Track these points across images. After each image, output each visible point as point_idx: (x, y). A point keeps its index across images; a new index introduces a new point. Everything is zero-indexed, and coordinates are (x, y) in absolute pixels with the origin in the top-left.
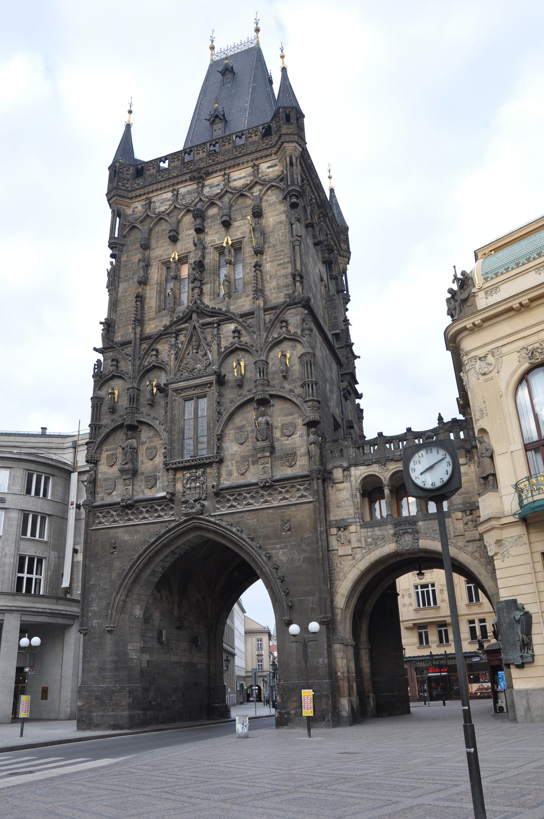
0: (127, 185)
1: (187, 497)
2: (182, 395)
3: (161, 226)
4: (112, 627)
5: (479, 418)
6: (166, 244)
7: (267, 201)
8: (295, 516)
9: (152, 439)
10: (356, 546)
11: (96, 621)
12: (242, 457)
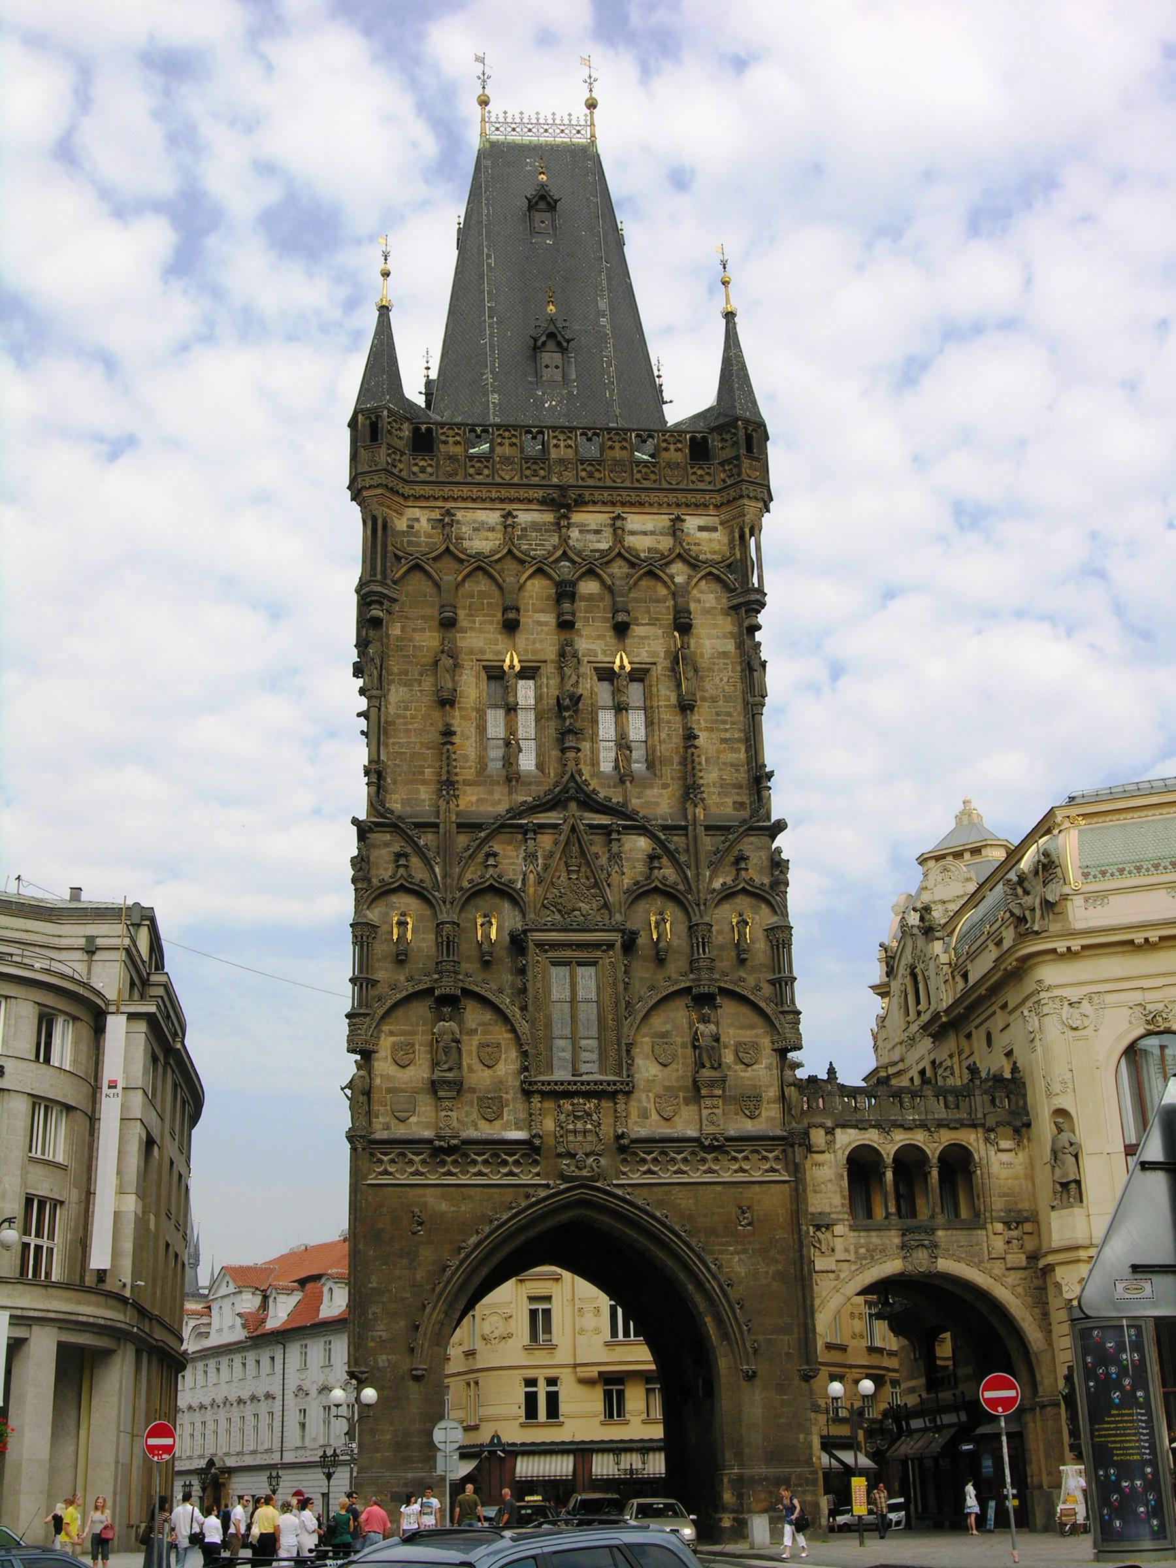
0: (401, 466)
2: (550, 954)
3: (478, 583)
4: (425, 1370)
5: (1059, 1092)
6: (491, 628)
7: (699, 601)
8: (759, 1202)
9: (491, 1028)
10: (843, 1259)
11: (384, 1357)
12: (667, 1088)
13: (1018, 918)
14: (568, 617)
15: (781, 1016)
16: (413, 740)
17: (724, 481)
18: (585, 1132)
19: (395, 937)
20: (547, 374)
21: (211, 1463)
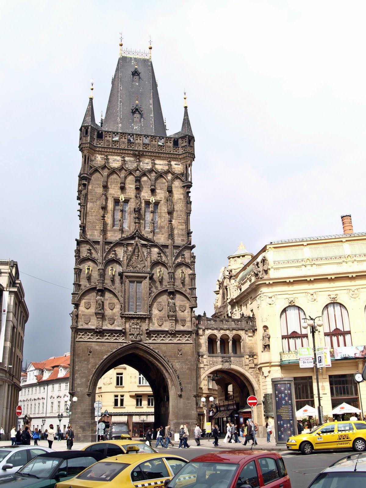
1: (133, 333)
8: (184, 349)
11: (79, 389)
13: (256, 274)
14: (138, 186)
15: (192, 299)
16: (93, 218)
17: (182, 152)
18: (137, 328)
19: (86, 272)
20: (135, 120)
21: (26, 416)
